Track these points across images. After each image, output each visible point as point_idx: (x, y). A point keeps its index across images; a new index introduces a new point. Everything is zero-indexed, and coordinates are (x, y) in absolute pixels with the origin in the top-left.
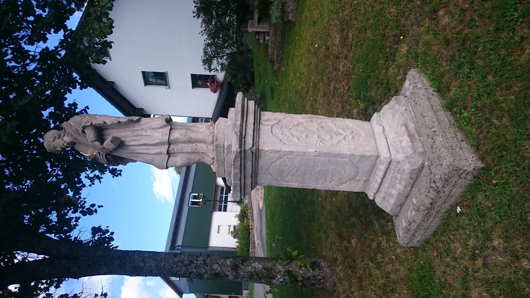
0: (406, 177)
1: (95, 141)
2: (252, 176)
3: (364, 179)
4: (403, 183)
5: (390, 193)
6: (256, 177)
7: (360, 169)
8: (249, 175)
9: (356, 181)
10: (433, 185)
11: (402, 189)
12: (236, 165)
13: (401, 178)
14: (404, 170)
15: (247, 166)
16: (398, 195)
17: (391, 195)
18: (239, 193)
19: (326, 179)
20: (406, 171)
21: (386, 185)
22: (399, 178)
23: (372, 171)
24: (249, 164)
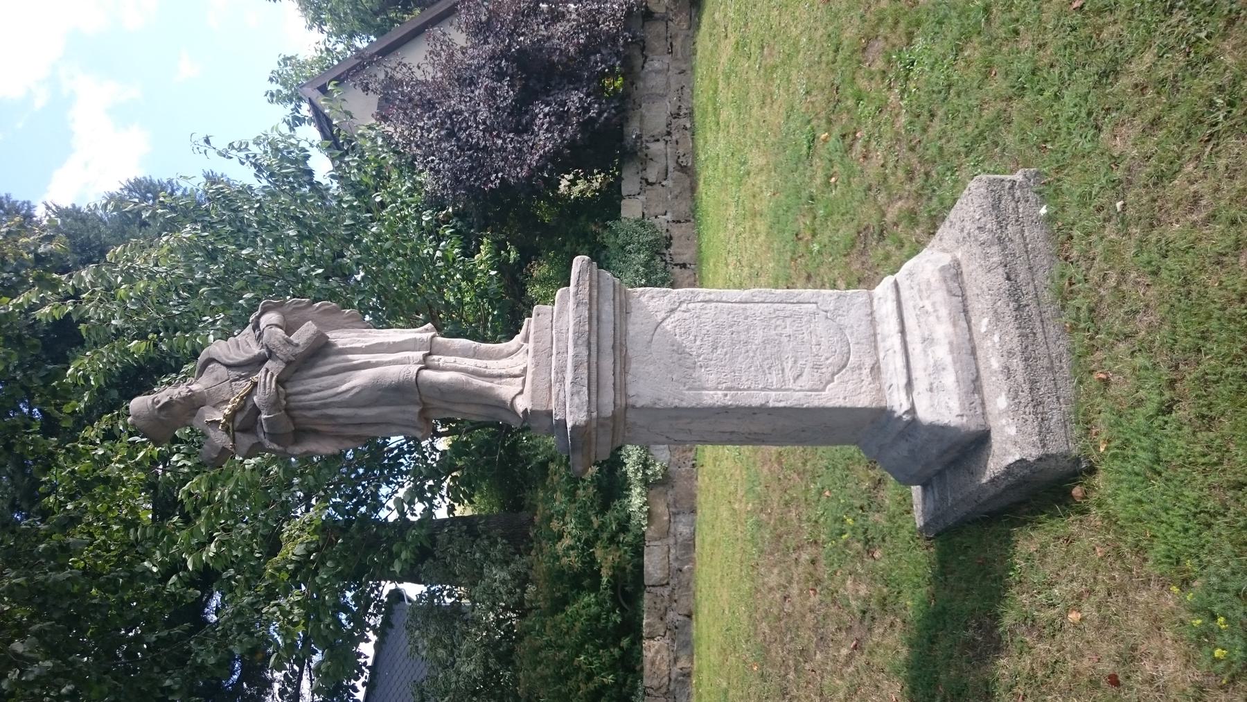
0: (940, 295)
1: (277, 326)
2: (614, 347)
3: (868, 362)
4: (944, 312)
5: (936, 362)
6: (625, 371)
7: (847, 332)
8: (607, 343)
9: (853, 369)
10: (983, 237)
11: (951, 329)
12: (580, 296)
13: (933, 304)
14: (928, 283)
15: (604, 317)
16: (951, 352)
17: (938, 368)
18: (585, 389)
19: (783, 370)
20: (933, 280)
21: (916, 348)
22: (929, 308)
23: (875, 335)
24: (608, 330)
